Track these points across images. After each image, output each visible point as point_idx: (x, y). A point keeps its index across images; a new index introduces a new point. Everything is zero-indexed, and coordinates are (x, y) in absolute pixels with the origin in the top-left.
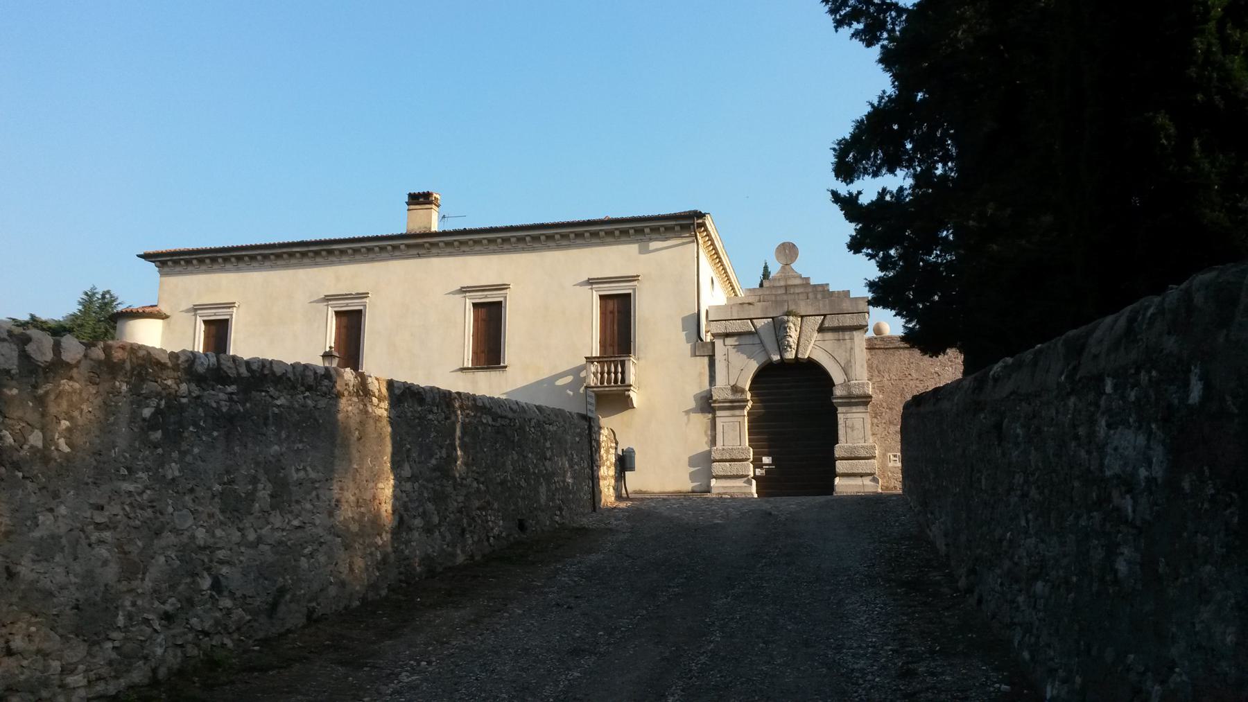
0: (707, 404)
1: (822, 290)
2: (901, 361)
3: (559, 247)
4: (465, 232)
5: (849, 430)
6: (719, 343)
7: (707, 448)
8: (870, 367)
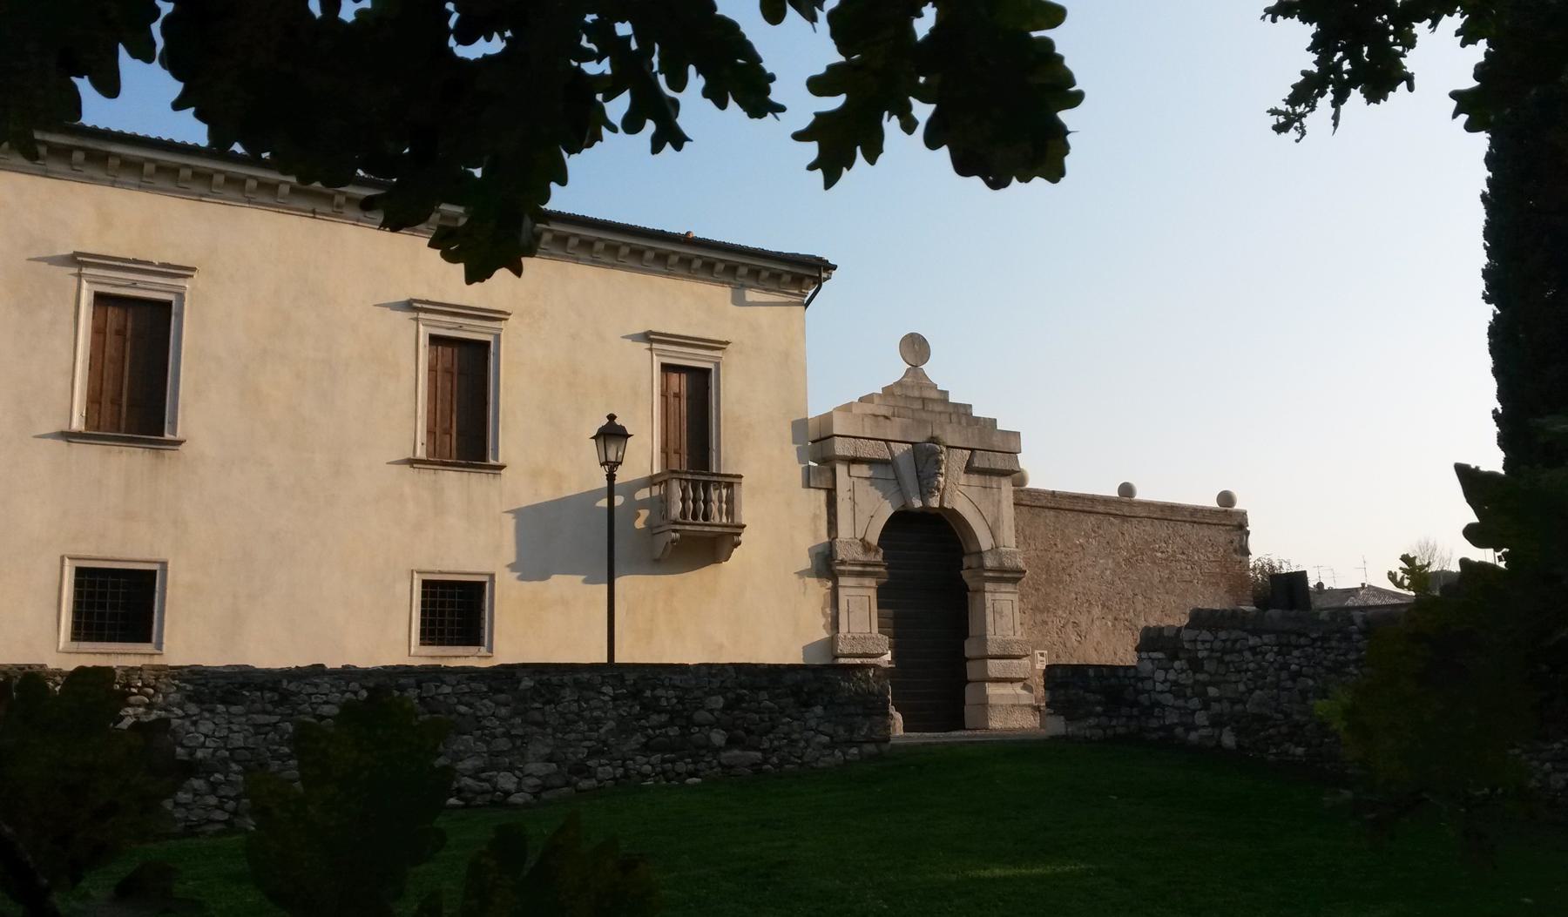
0: (826, 565)
2: (1046, 525)
3: (595, 262)
6: (841, 469)
7: (823, 634)
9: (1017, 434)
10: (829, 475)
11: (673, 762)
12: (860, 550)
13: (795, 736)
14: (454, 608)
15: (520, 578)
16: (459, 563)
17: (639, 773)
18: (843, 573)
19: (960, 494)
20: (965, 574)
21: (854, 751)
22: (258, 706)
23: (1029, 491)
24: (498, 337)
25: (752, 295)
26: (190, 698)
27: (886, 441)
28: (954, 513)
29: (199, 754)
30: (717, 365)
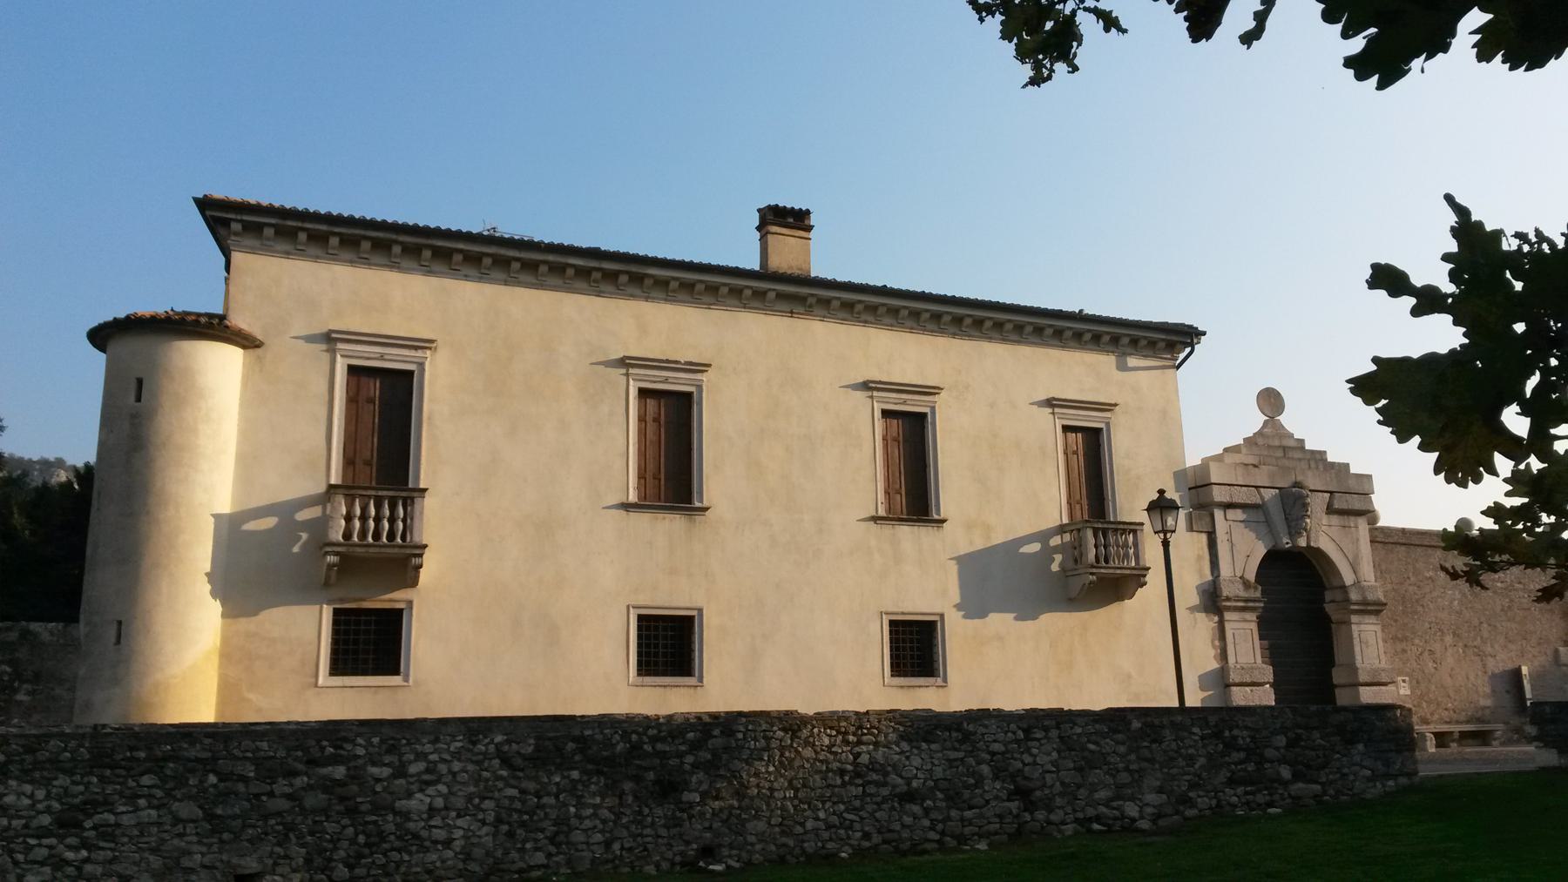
0: (1213, 600)
3: (1004, 340)
4: (884, 291)
6: (1218, 514)
9: (1369, 477)
10: (1208, 519)
11: (1252, 793)
13: (1346, 770)
14: (915, 646)
15: (965, 617)
16: (917, 603)
17: (1229, 804)
18: (1229, 609)
19: (1324, 534)
20: (1328, 608)
21: (1391, 783)
22: (948, 744)
23: (1383, 529)
24: (933, 408)
25: (1132, 361)
26: (902, 737)
28: (1318, 551)
29: (915, 784)
30: (1108, 424)
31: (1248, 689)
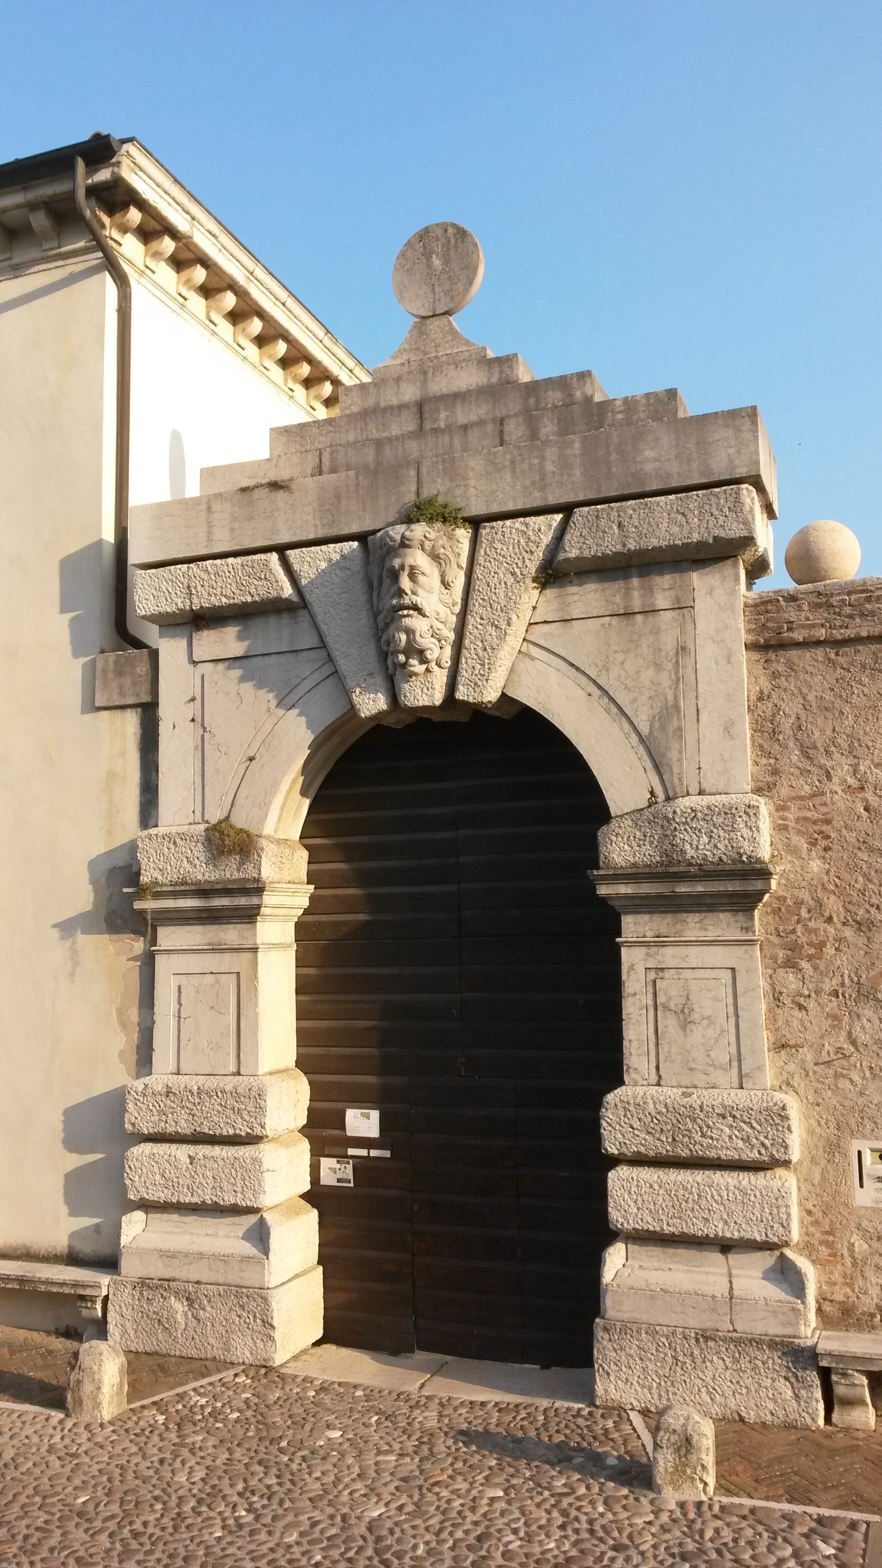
1: (567, 407)
5: (669, 1024)
6: (171, 651)
8: (767, 730)
12: (199, 851)
27: (281, 549)
31: (182, 1152)
